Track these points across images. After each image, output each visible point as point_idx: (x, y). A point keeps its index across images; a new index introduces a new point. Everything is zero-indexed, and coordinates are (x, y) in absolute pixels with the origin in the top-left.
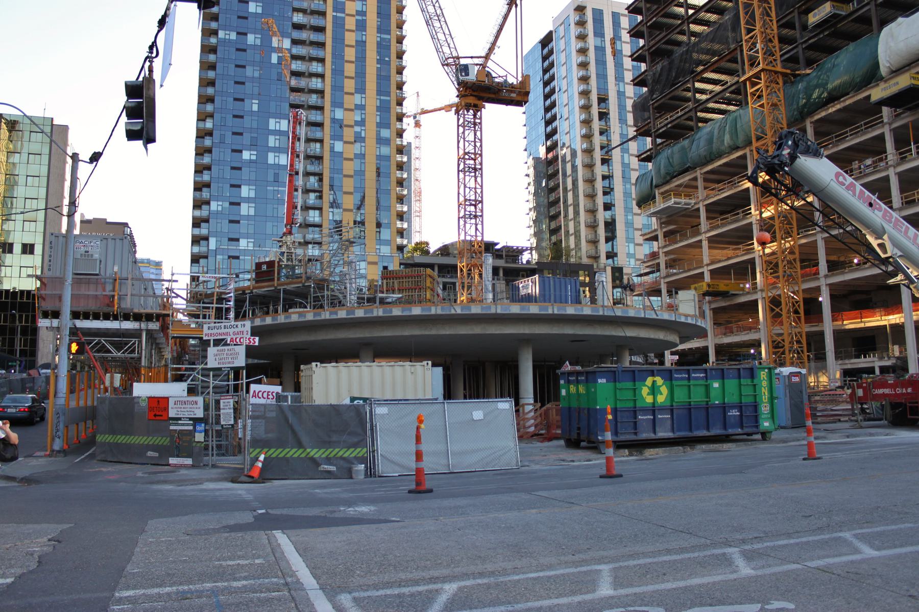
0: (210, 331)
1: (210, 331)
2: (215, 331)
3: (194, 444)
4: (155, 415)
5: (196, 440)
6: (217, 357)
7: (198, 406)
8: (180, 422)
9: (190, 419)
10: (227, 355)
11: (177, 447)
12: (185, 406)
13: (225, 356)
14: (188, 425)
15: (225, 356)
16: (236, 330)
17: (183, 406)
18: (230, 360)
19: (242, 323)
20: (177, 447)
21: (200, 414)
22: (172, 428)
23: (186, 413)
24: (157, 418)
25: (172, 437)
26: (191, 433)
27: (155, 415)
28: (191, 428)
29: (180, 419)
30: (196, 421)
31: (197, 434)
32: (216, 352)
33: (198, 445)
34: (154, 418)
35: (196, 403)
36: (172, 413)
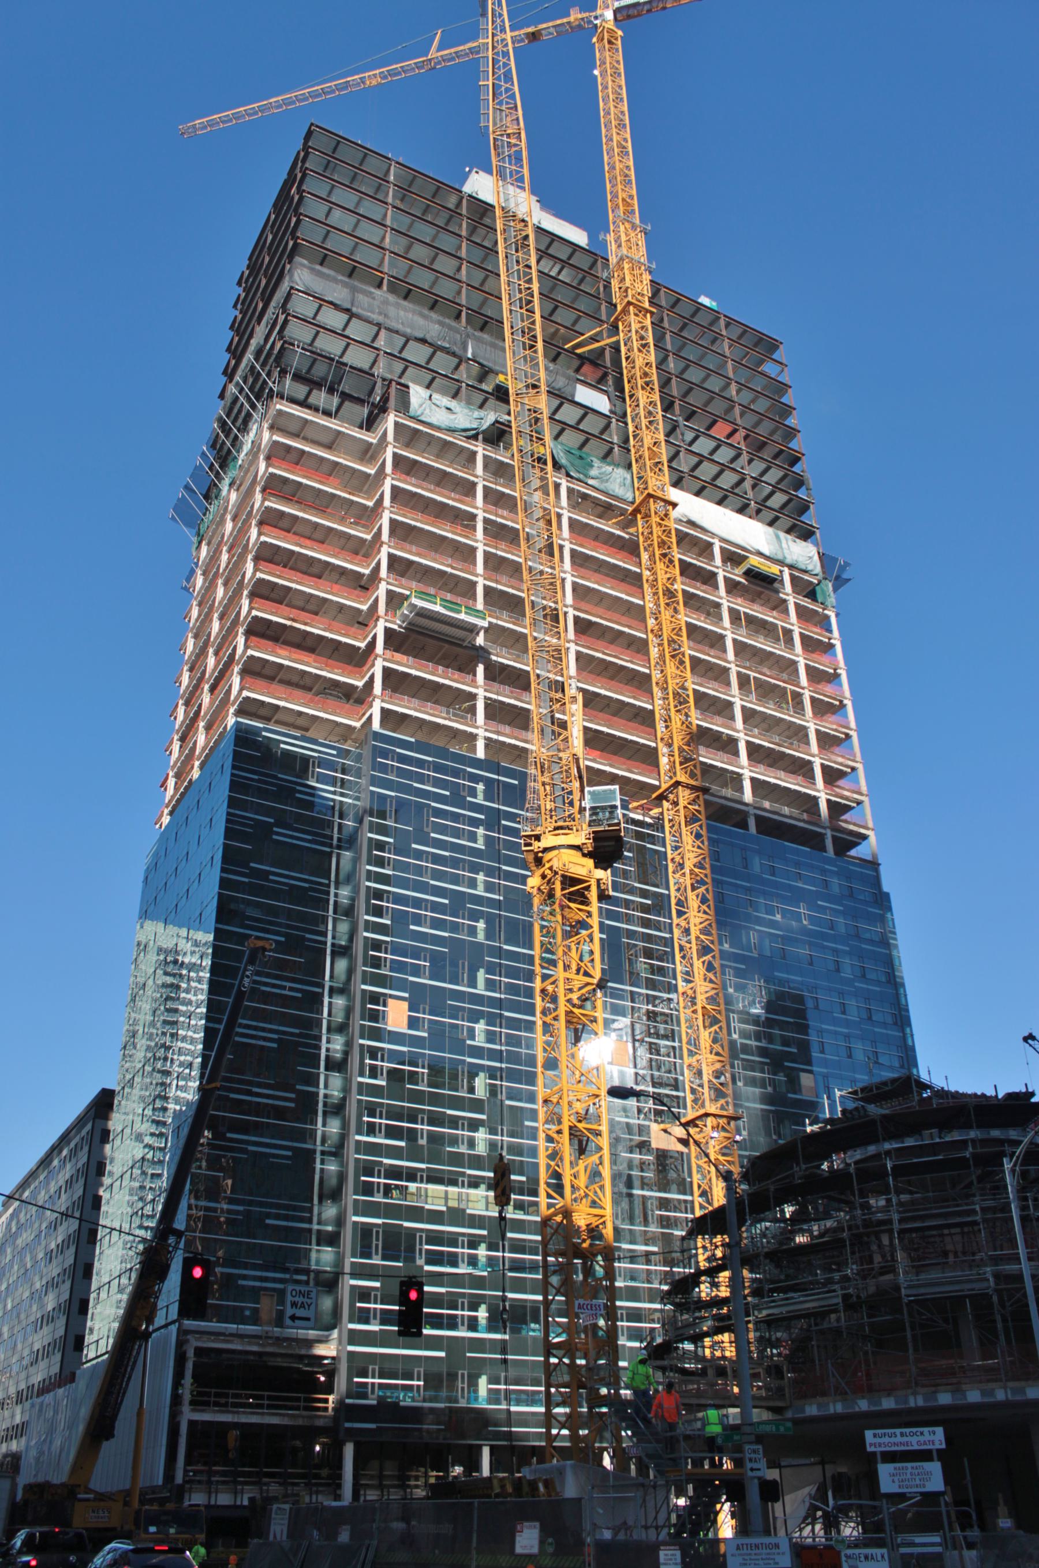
0: (878, 1440)
1: (878, 1440)
2: (886, 1440)
6: (896, 1479)
7: (781, 1550)
10: (911, 1474)
12: (757, 1551)
13: (909, 1476)
15: (909, 1476)
16: (921, 1438)
18: (918, 1482)
32: (892, 1471)
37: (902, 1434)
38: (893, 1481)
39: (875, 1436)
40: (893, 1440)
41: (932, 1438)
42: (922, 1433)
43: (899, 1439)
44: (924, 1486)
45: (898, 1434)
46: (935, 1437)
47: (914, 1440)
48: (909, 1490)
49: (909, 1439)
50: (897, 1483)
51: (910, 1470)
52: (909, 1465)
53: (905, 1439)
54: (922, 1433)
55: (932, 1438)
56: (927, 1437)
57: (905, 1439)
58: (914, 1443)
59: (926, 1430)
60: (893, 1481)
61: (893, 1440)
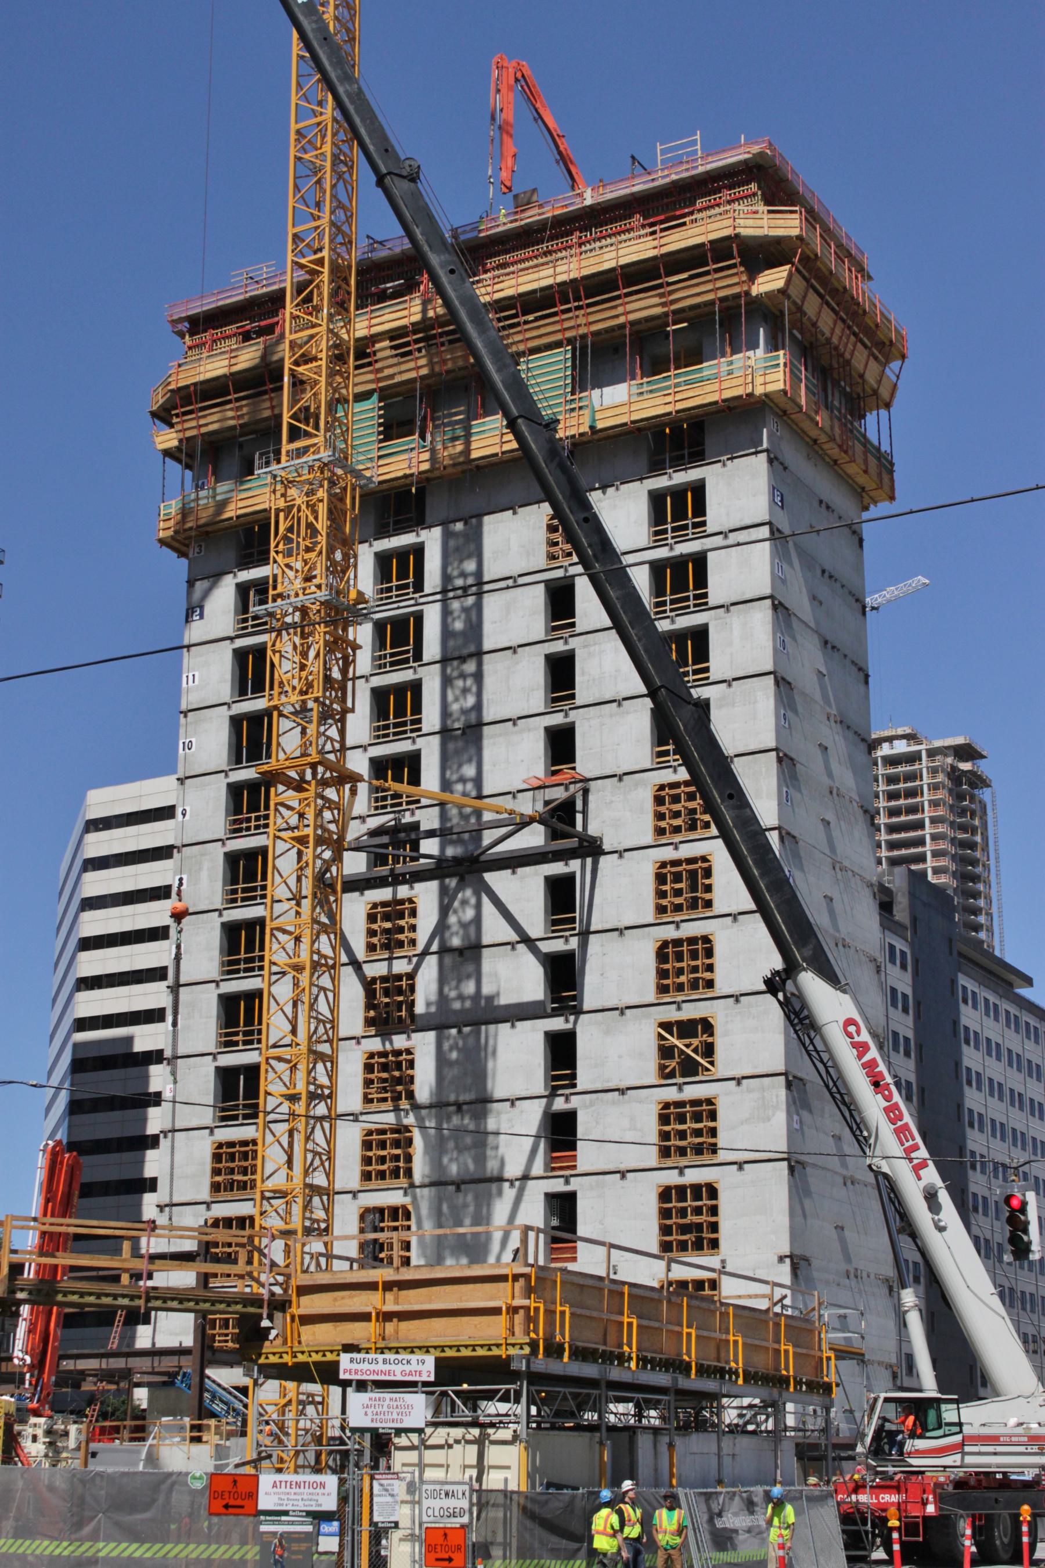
0: (355, 1366)
1: (355, 1366)
2: (365, 1366)
3: (316, 1556)
4: (226, 1506)
5: (321, 1549)
6: (369, 1411)
8: (284, 1518)
9: (309, 1513)
10: (388, 1407)
11: (276, 1562)
13: (385, 1409)
14: (302, 1523)
15: (385, 1409)
17: (294, 1490)
18: (395, 1416)
19: (420, 1357)
20: (276, 1562)
21: (330, 1503)
22: (263, 1528)
23: (301, 1503)
24: (231, 1510)
25: (265, 1546)
26: (312, 1538)
27: (226, 1506)
28: (309, 1528)
29: (286, 1513)
30: (319, 1517)
31: (322, 1539)
32: (367, 1402)
33: (324, 1557)
34: (224, 1511)
35: (323, 1485)
36: (265, 1502)
37: (385, 1361)
38: (366, 1414)
39: (352, 1361)
40: (373, 1367)
41: (420, 1367)
42: (408, 1362)
43: (381, 1366)
44: (402, 1421)
45: (381, 1361)
46: (425, 1367)
47: (398, 1368)
48: (384, 1425)
49: (392, 1367)
50: (370, 1416)
51: (387, 1402)
52: (388, 1396)
53: (387, 1367)
54: (408, 1362)
55: (420, 1367)
56: (414, 1366)
57: (387, 1367)
58: (398, 1373)
59: (414, 1358)
60: (366, 1414)
61: (373, 1367)
